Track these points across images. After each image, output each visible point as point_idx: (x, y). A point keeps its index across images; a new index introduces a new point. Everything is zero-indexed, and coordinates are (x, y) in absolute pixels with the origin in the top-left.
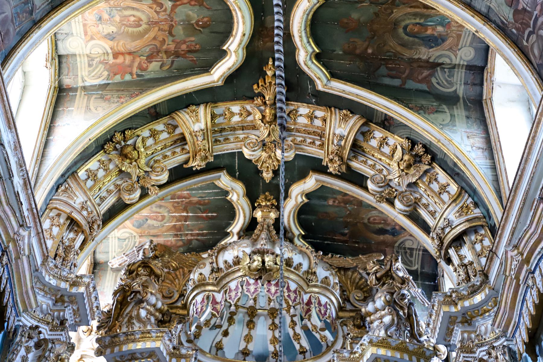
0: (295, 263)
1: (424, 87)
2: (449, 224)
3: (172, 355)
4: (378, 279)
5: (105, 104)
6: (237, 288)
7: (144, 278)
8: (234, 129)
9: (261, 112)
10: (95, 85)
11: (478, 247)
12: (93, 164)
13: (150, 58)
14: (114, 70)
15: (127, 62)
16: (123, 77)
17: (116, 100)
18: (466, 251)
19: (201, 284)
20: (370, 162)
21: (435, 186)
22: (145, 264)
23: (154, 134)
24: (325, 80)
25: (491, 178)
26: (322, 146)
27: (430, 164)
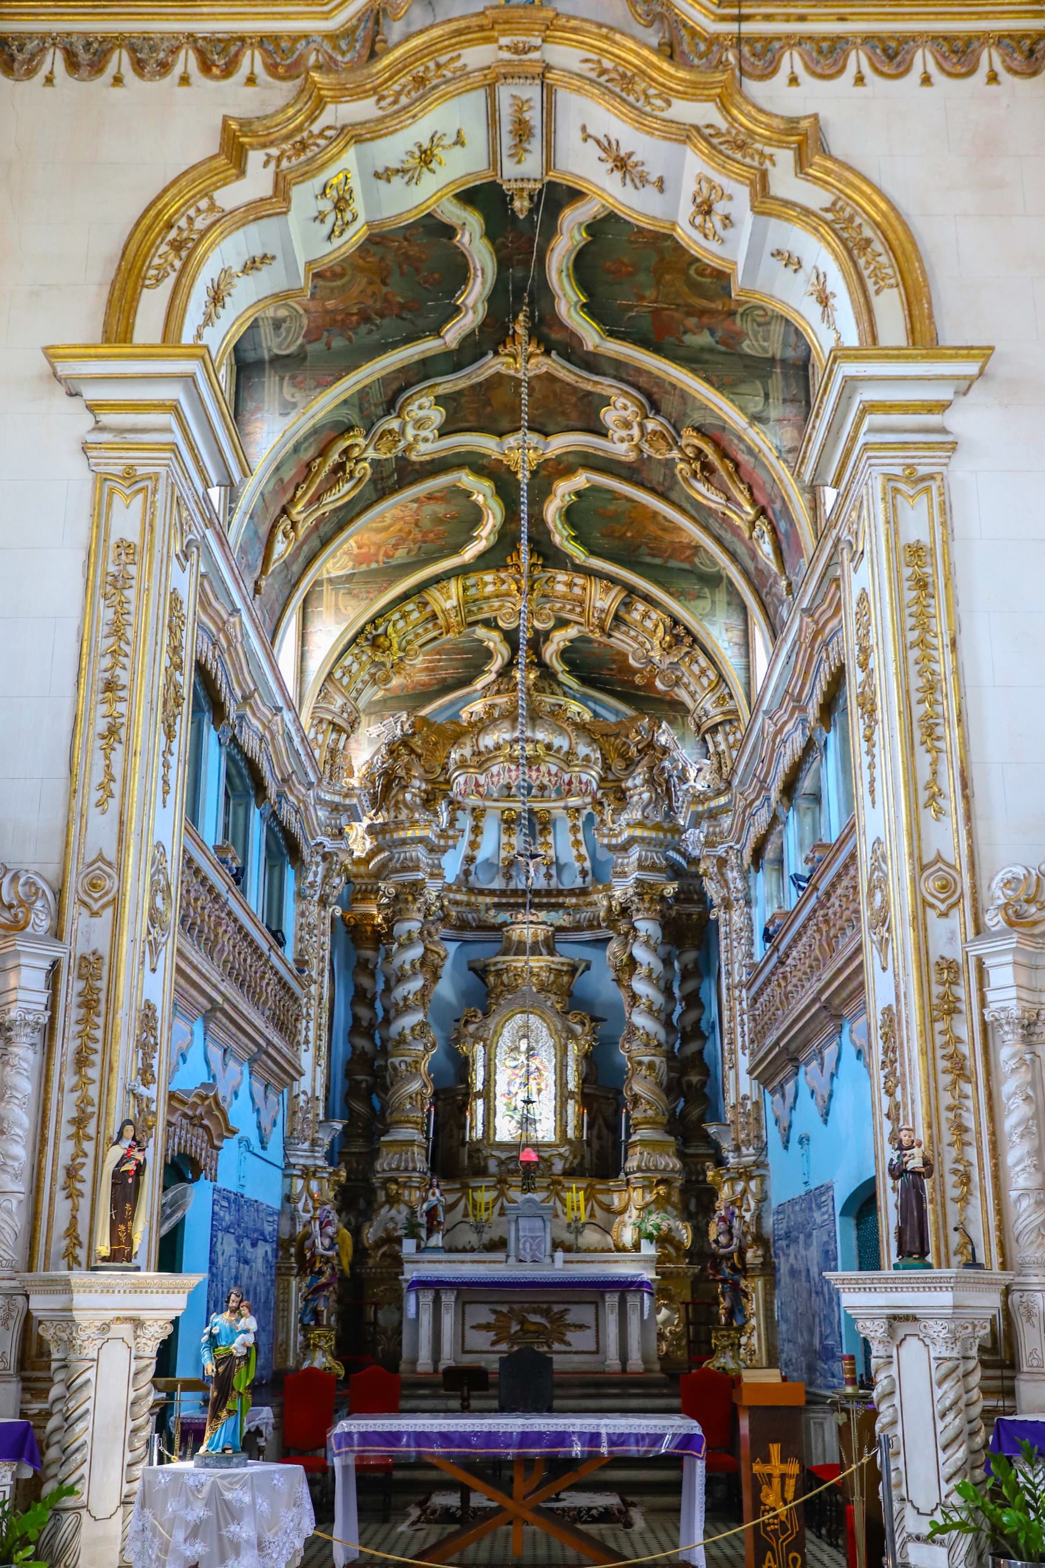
0: (556, 745)
1: (686, 566)
2: (706, 714)
3: (439, 837)
4: (639, 751)
5: (354, 602)
6: (499, 774)
7: (406, 758)
8: (487, 598)
9: (517, 582)
10: (341, 577)
11: (731, 738)
12: (348, 660)
13: (395, 547)
14: (358, 560)
15: (372, 551)
16: (368, 565)
17: (364, 595)
18: (720, 737)
19: (463, 764)
20: (633, 633)
21: (695, 668)
22: (405, 742)
23: (404, 616)
24: (583, 557)
25: (743, 680)
26: (581, 614)
27: (691, 646)
